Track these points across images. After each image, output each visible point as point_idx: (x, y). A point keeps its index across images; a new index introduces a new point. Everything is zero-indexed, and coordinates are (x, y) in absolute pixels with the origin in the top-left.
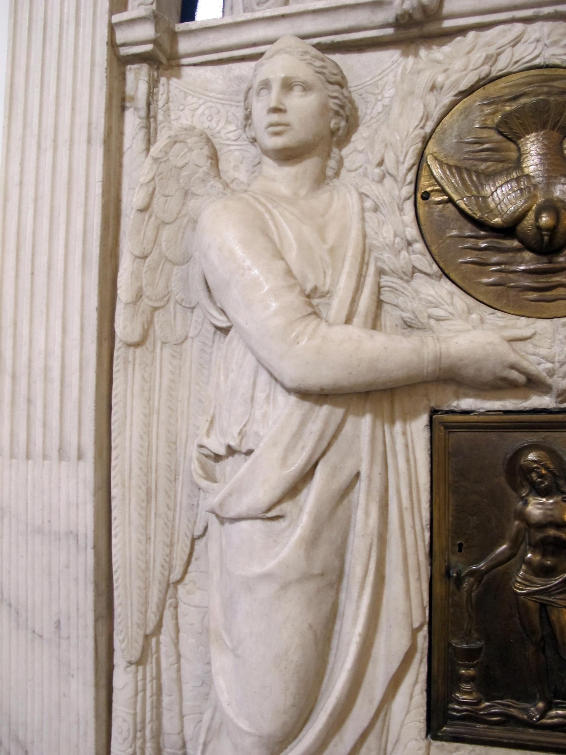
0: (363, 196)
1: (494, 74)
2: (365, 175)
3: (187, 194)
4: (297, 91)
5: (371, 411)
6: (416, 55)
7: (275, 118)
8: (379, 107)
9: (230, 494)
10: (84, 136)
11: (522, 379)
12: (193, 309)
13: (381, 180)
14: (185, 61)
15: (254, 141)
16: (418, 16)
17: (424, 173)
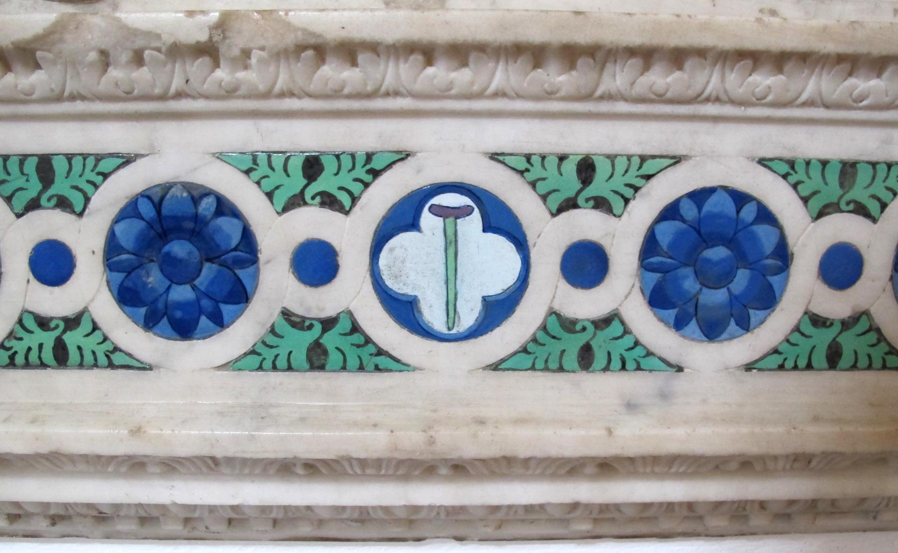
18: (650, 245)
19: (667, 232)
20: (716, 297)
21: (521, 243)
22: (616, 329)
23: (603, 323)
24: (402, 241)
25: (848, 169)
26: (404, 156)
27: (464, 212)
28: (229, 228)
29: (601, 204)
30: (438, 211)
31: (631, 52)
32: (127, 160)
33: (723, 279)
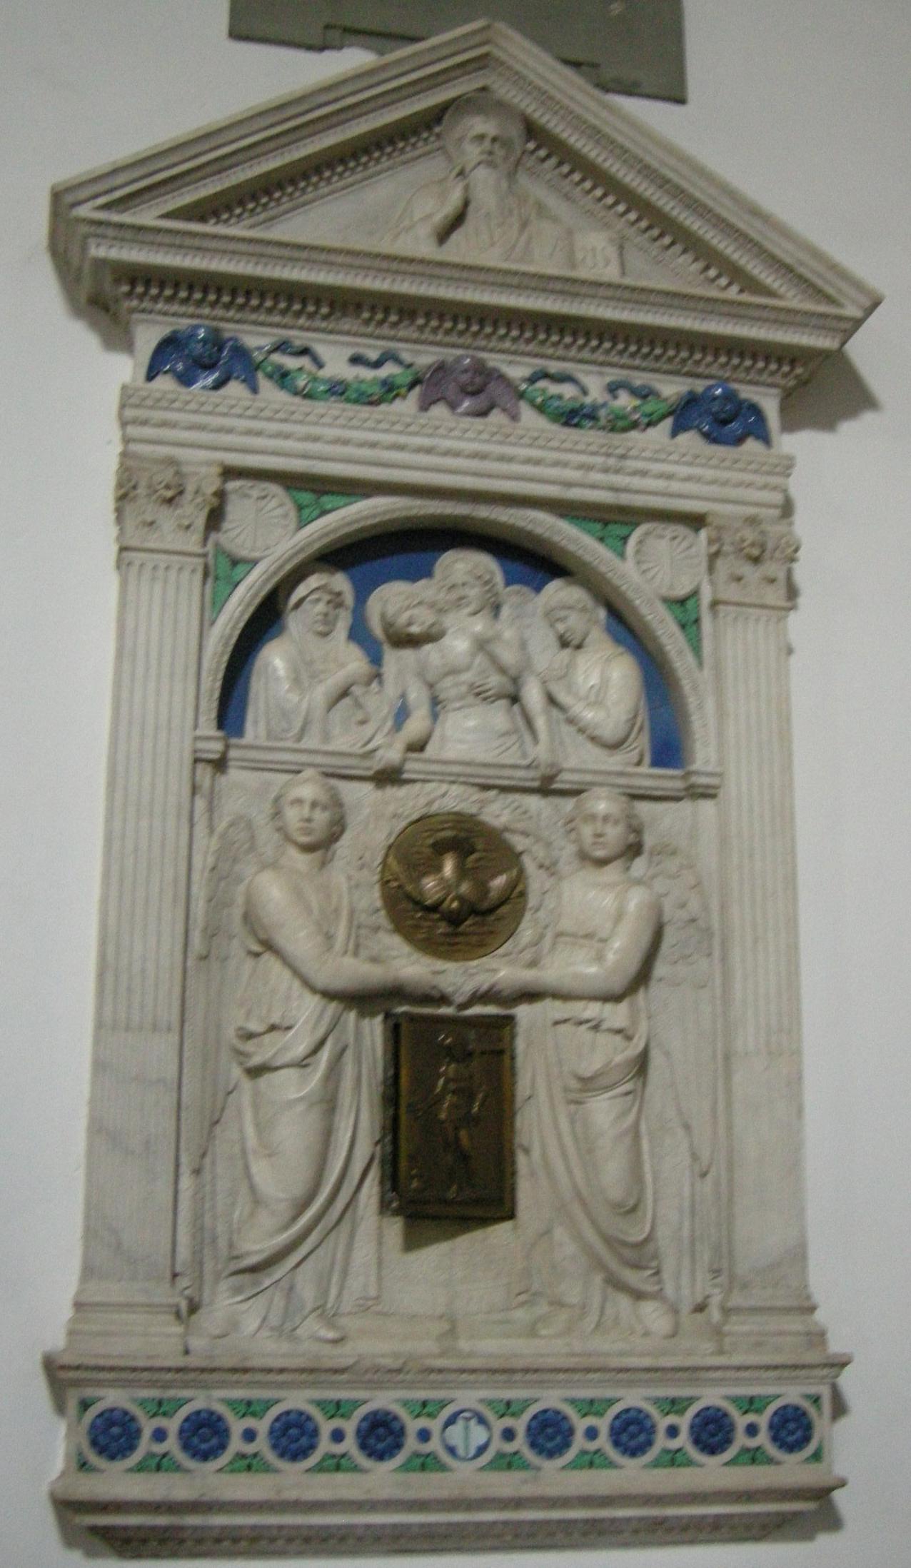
0: (349, 878)
1: (431, 813)
3: (235, 860)
7: (306, 825)
15: (279, 829)
19: (534, 1424)
24: (450, 1428)
25: (592, 1402)
26: (452, 1401)
32: (365, 1402)
33: (551, 1438)
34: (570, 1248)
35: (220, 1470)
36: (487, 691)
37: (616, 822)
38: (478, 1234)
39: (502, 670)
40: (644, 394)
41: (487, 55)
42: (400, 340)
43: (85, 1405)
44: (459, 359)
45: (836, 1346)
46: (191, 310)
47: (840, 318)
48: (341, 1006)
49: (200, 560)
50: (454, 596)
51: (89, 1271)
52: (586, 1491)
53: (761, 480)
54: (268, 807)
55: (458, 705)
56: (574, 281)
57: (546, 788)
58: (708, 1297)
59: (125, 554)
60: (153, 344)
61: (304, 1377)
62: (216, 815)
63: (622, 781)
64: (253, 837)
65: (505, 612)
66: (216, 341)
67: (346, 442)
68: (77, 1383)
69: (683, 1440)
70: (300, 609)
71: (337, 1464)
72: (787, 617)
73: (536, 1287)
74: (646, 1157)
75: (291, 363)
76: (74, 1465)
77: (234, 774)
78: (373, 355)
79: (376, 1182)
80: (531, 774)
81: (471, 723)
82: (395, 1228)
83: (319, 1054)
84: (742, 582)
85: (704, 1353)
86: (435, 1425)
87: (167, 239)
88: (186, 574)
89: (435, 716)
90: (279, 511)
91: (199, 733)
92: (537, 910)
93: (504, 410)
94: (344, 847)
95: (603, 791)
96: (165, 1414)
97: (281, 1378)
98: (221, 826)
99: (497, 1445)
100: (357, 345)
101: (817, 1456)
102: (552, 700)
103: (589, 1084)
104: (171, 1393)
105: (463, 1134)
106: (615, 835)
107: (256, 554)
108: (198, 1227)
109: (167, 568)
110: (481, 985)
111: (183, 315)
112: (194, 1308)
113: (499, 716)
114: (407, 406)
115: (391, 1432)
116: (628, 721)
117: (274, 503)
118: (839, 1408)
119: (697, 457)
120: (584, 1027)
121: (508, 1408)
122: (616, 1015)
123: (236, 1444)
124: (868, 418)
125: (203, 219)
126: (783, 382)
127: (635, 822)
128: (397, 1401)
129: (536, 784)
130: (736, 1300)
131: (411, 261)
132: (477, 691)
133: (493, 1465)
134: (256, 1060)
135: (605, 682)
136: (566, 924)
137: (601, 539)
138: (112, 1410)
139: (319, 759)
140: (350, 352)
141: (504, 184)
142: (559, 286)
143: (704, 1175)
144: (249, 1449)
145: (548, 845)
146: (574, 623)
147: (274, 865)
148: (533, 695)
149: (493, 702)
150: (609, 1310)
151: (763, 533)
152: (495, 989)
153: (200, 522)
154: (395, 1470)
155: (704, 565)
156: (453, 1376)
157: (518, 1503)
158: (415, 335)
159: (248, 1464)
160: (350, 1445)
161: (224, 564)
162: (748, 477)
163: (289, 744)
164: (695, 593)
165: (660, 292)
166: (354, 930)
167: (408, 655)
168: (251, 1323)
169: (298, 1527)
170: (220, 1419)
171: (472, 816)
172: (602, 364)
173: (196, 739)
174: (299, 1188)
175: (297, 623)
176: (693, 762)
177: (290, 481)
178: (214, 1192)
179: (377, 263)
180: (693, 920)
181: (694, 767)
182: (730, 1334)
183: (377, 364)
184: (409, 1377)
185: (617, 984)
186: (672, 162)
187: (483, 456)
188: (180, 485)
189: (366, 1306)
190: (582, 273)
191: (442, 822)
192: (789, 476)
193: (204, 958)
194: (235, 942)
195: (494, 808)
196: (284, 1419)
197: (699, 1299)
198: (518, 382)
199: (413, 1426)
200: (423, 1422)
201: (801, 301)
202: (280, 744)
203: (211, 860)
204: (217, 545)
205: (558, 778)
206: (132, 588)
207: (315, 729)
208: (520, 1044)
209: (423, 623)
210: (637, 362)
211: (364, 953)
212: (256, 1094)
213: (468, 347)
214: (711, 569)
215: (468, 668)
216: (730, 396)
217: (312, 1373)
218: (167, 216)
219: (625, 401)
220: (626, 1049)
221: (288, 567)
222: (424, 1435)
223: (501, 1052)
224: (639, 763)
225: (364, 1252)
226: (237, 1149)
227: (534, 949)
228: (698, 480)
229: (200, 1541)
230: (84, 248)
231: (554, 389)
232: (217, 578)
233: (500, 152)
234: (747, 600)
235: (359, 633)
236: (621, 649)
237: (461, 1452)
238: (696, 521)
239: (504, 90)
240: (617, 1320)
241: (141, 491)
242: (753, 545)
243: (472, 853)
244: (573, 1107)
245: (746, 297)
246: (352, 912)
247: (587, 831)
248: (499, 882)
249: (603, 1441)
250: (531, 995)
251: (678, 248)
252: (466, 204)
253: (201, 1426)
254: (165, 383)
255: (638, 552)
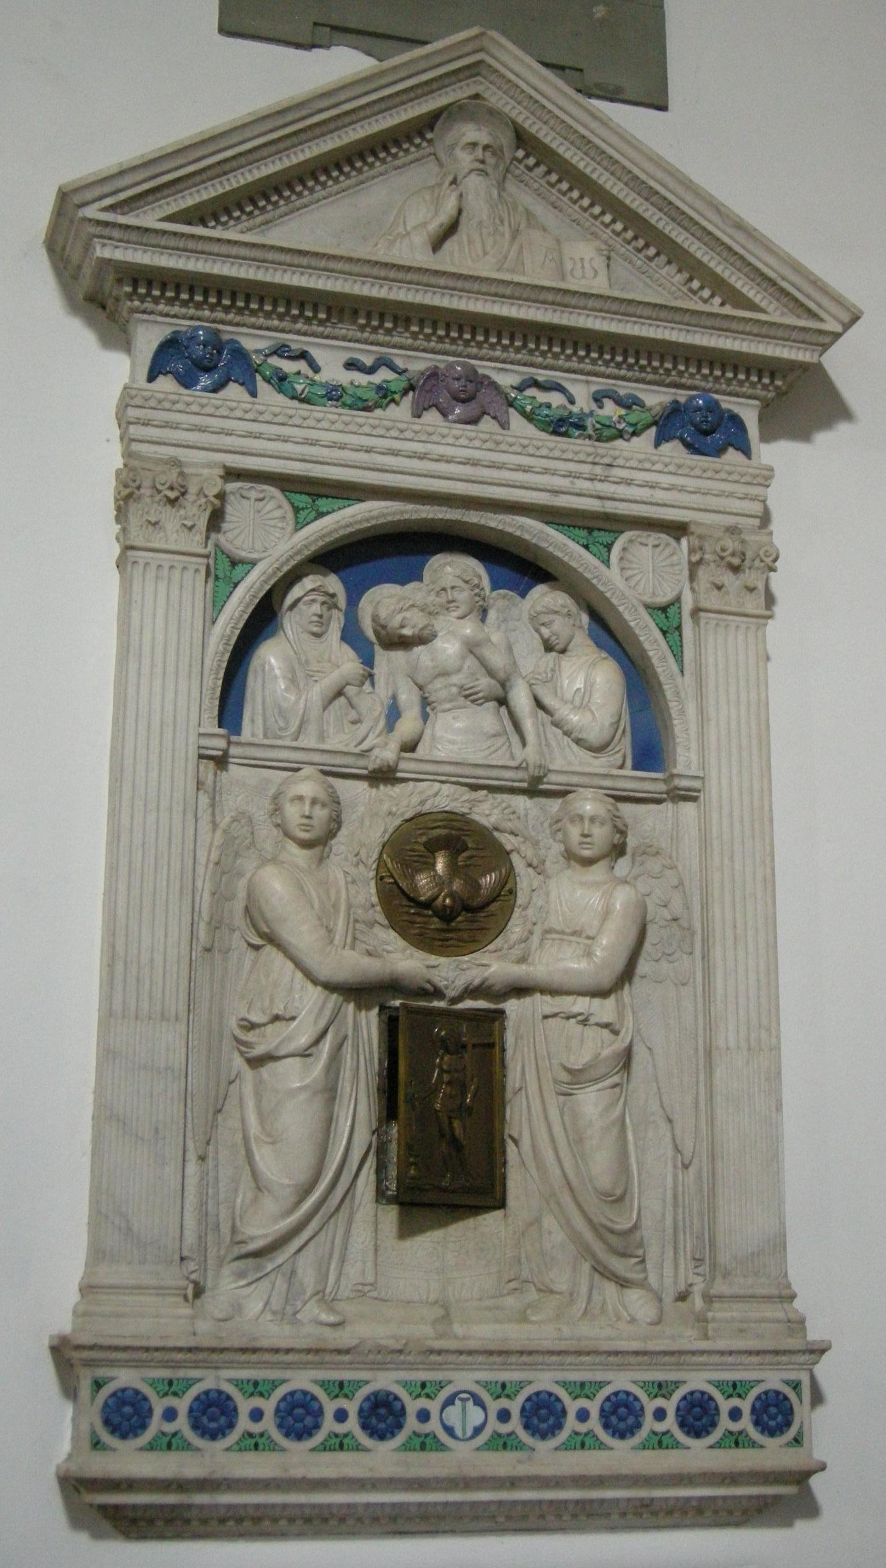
0: (346, 873)
2: (346, 859)
3: (237, 855)
4: (318, 807)
5: (355, 1000)
6: (377, 787)
8: (354, 817)
9: (282, 1041)
10: (181, 808)
11: (432, 989)
12: (234, 930)
13: (358, 864)
14: (231, 760)
15: (277, 826)
16: (385, 769)
17: (382, 864)
18: (523, 1409)
19: (528, 1405)
20: (544, 1426)
21: (484, 1408)
22: (514, 1436)
23: (509, 1435)
24: (450, 1409)
25: (583, 1385)
26: (450, 1382)
27: (468, 1399)
28: (397, 1405)
29: (508, 1396)
30: (462, 1400)
31: (518, 1352)
32: (367, 1382)
33: (545, 1420)
34: (559, 1236)
35: (228, 1449)
36: (477, 693)
37: (603, 824)
38: (471, 1222)
39: (491, 673)
40: (628, 403)
41: (481, 62)
42: (394, 347)
43: (98, 1385)
44: (451, 366)
45: (815, 1334)
46: (191, 311)
47: (821, 332)
48: (341, 998)
49: (204, 561)
50: (443, 599)
51: (97, 1254)
52: (578, 1471)
53: (741, 489)
54: (268, 805)
55: (448, 706)
56: (566, 292)
57: (534, 789)
58: (691, 1285)
59: (130, 553)
60: (155, 345)
61: (310, 1357)
62: (217, 811)
63: (608, 783)
64: (252, 833)
65: (492, 615)
66: (217, 344)
67: (343, 447)
68: (89, 1363)
69: (670, 1423)
70: (296, 609)
71: (340, 1443)
72: (766, 625)
73: (525, 1274)
74: (631, 1147)
75: (288, 367)
76: (86, 1444)
77: (235, 771)
78: (368, 361)
79: (373, 1171)
80: (520, 775)
81: (458, 725)
82: (390, 1215)
83: (321, 1044)
84: (724, 589)
85: (689, 1339)
86: (434, 1406)
87: (173, 242)
88: (189, 574)
89: (425, 717)
90: (278, 513)
91: (202, 730)
92: (525, 908)
93: (494, 418)
94: (340, 844)
95: (589, 793)
96: (175, 1394)
97: (290, 1358)
98: (224, 822)
99: (494, 1425)
100: (350, 349)
101: (797, 1441)
102: (539, 704)
103: (577, 1077)
104: (181, 1373)
105: (456, 1124)
106: (601, 834)
107: (254, 556)
108: (203, 1215)
109: (172, 567)
110: (473, 980)
111: (184, 317)
112: (199, 1292)
113: (488, 718)
114: (401, 411)
115: (391, 1412)
116: (612, 724)
117: (271, 505)
118: (817, 1398)
119: (679, 466)
120: (573, 1021)
121: (503, 1390)
122: (604, 1010)
123: (244, 1423)
124: (843, 429)
125: (203, 222)
126: (764, 393)
127: (620, 824)
128: (398, 1382)
129: (525, 785)
130: (720, 1287)
131: (409, 269)
132: (467, 692)
133: (489, 1446)
134: (259, 1050)
135: (589, 685)
136: (554, 922)
137: (586, 547)
138: (123, 1390)
139: (317, 758)
140: (346, 356)
141: (495, 192)
142: (550, 297)
143: (686, 1167)
144: (256, 1428)
145: (536, 844)
146: (559, 627)
147: (274, 860)
148: (521, 699)
149: (481, 704)
150: (596, 1297)
151: (743, 542)
152: (486, 984)
153: (203, 522)
154: (397, 1450)
155: (686, 573)
156: (451, 1358)
157: (513, 1483)
158: (410, 341)
159: (255, 1443)
160: (352, 1424)
161: (225, 564)
162: (728, 487)
163: (288, 743)
164: (678, 599)
165: (648, 304)
166: (351, 925)
167: (399, 657)
168: (254, 1307)
169: (301, 1506)
170: (229, 1398)
171: (463, 815)
172: (589, 374)
173: (200, 735)
174: (302, 1175)
175: (293, 624)
176: (675, 767)
177: (286, 483)
178: (217, 1178)
179: (375, 271)
180: (675, 920)
181: (675, 771)
182: (714, 1319)
183: (371, 370)
184: (410, 1358)
185: (606, 979)
186: (660, 175)
187: (475, 463)
188: (183, 487)
189: (361, 1292)
190: (572, 285)
191: (435, 821)
192: (768, 486)
193: (208, 950)
194: (237, 934)
195: (485, 807)
196: (289, 1398)
197: (682, 1287)
198: (509, 390)
199: (412, 1406)
200: (423, 1403)
201: (783, 314)
202: (279, 742)
203: (214, 857)
204: (217, 546)
205: (545, 780)
206: (136, 588)
207: (312, 728)
208: (510, 1039)
209: (414, 627)
210: (623, 372)
211: (361, 947)
212: (259, 1084)
213: (459, 355)
214: (692, 577)
215: (459, 670)
216: (713, 407)
217: (317, 1353)
218: (169, 219)
219: (610, 410)
220: (614, 1041)
221: (285, 569)
222: (424, 1416)
223: (491, 1045)
224: (621, 767)
225: (361, 1237)
226: (239, 1137)
227: (523, 945)
228: (682, 489)
229: (204, 1522)
230: (88, 248)
231: (542, 397)
232: (217, 578)
233: (491, 160)
234: (727, 608)
235: (351, 635)
236: (604, 655)
237: (459, 1432)
238: (678, 530)
239: (496, 99)
240: (603, 1310)
241: (146, 491)
242: (733, 554)
243: (464, 851)
244: (562, 1098)
245: (728, 310)
246: (349, 906)
247: (574, 832)
248: (488, 880)
249: (594, 1423)
250: (521, 990)
251: (663, 258)
252: (460, 212)
253: (210, 1406)
254: (166, 384)
255: (621, 559)
